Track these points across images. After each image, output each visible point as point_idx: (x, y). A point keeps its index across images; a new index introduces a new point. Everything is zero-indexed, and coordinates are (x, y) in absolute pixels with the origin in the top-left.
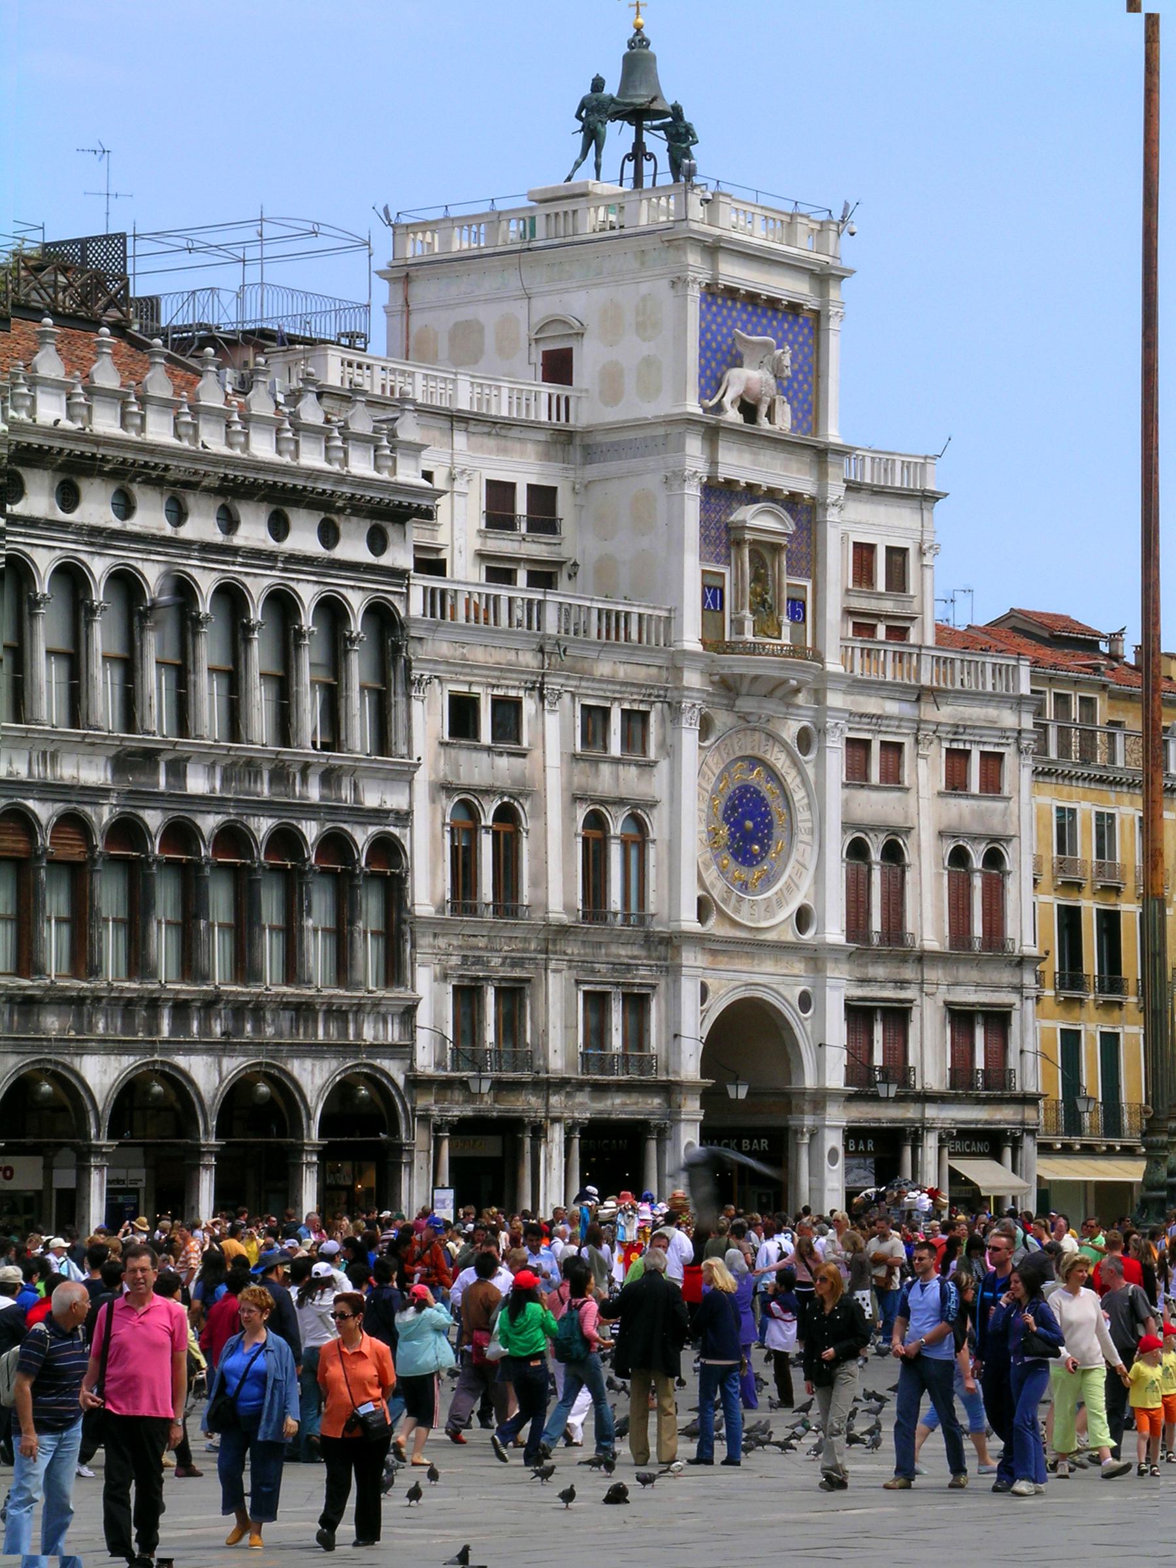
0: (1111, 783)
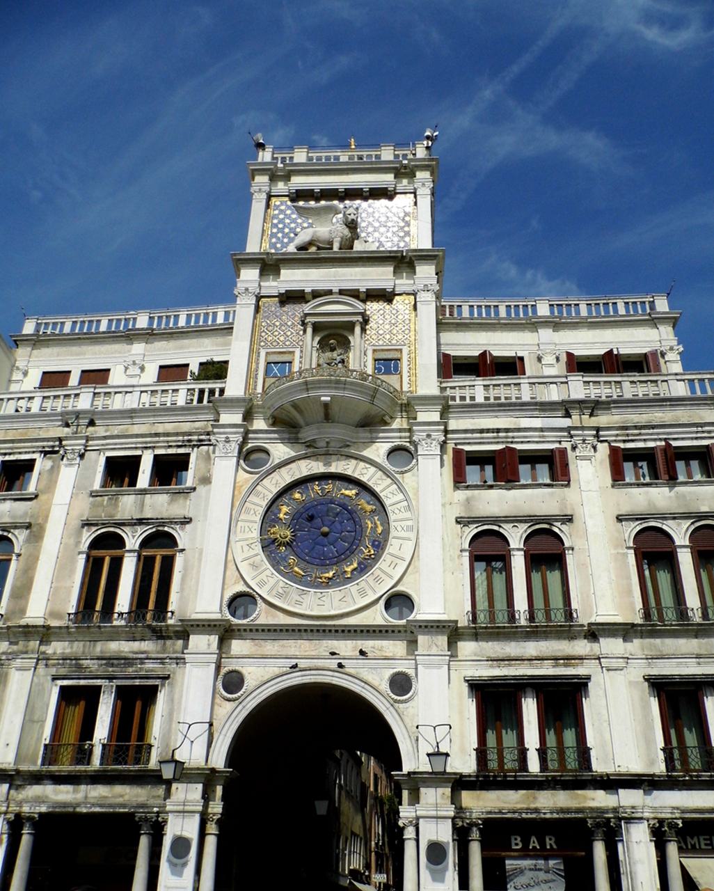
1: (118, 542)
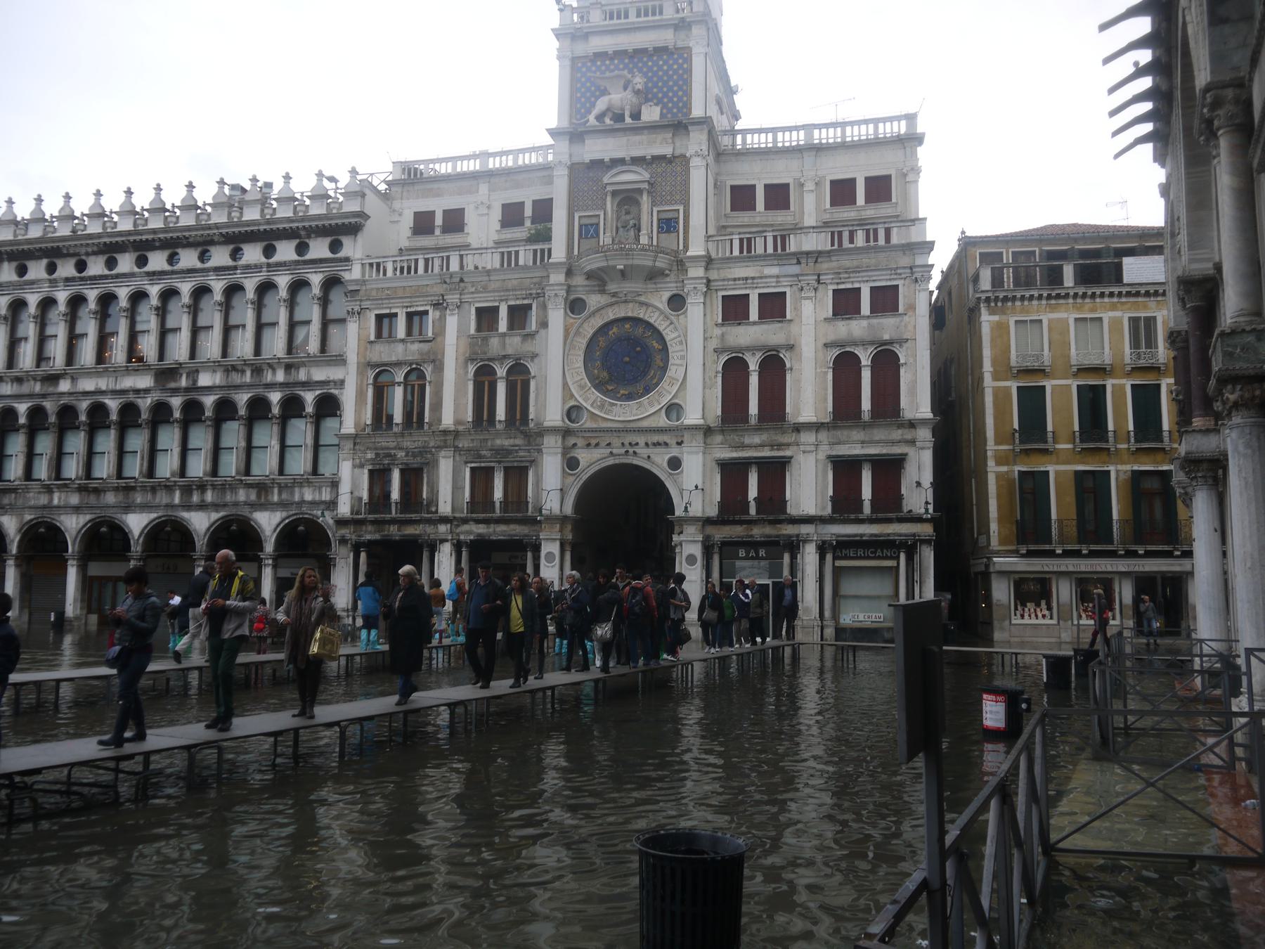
0: (1147, 294)
1: (494, 372)
